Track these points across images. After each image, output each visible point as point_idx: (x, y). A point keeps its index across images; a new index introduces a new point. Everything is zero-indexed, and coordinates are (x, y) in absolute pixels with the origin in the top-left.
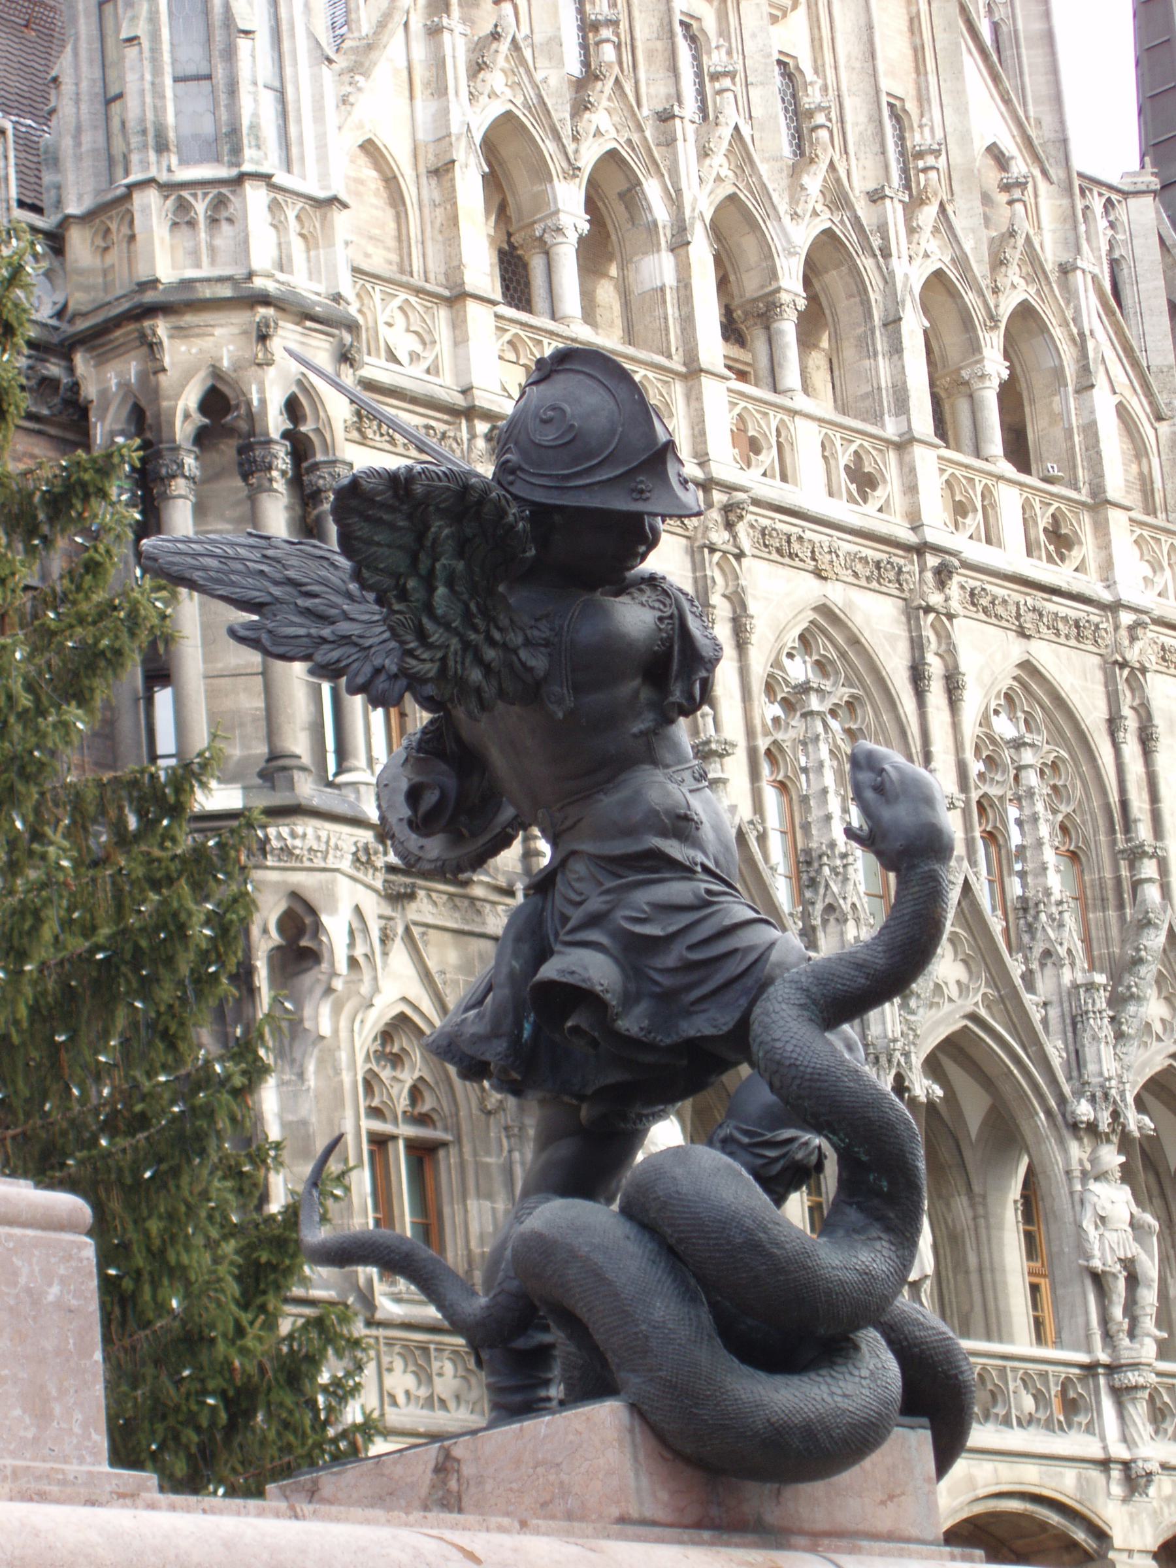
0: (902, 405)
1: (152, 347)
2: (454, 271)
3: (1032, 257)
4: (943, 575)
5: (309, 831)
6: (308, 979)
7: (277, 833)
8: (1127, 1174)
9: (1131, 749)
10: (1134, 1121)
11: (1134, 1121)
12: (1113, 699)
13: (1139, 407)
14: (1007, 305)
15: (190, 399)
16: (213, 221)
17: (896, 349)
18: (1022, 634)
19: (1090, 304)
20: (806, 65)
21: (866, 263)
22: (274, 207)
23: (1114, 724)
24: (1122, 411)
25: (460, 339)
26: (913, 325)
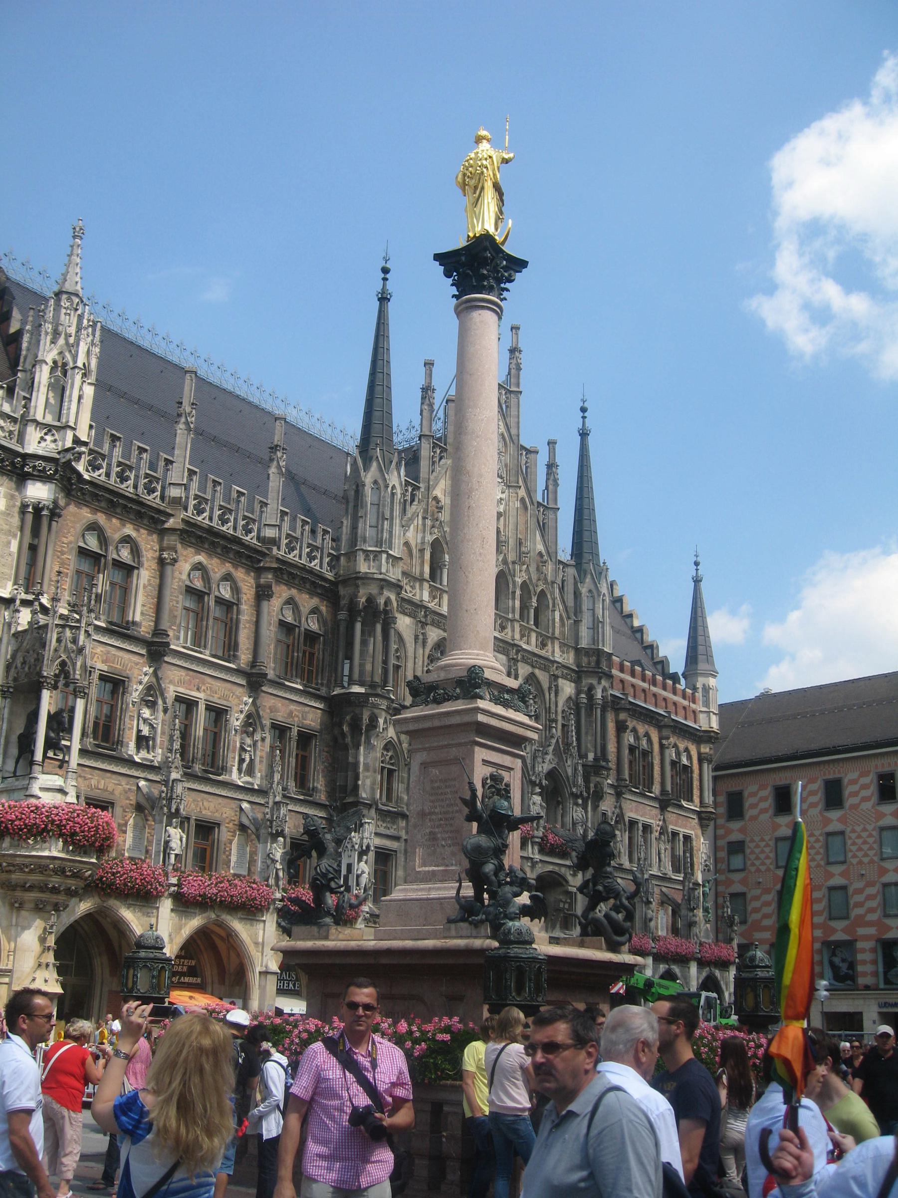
0: (513, 612)
1: (357, 586)
2: (422, 573)
3: (546, 579)
4: (518, 652)
5: (378, 701)
6: (372, 732)
7: (372, 699)
8: (540, 794)
9: (553, 695)
10: (544, 782)
11: (544, 782)
12: (550, 683)
13: (564, 615)
14: (539, 589)
15: (363, 600)
16: (374, 560)
17: (514, 599)
18: (533, 667)
19: (557, 591)
20: (502, 530)
21: (509, 578)
22: (387, 558)
23: (550, 688)
24: (561, 616)
25: (421, 589)
26: (518, 592)
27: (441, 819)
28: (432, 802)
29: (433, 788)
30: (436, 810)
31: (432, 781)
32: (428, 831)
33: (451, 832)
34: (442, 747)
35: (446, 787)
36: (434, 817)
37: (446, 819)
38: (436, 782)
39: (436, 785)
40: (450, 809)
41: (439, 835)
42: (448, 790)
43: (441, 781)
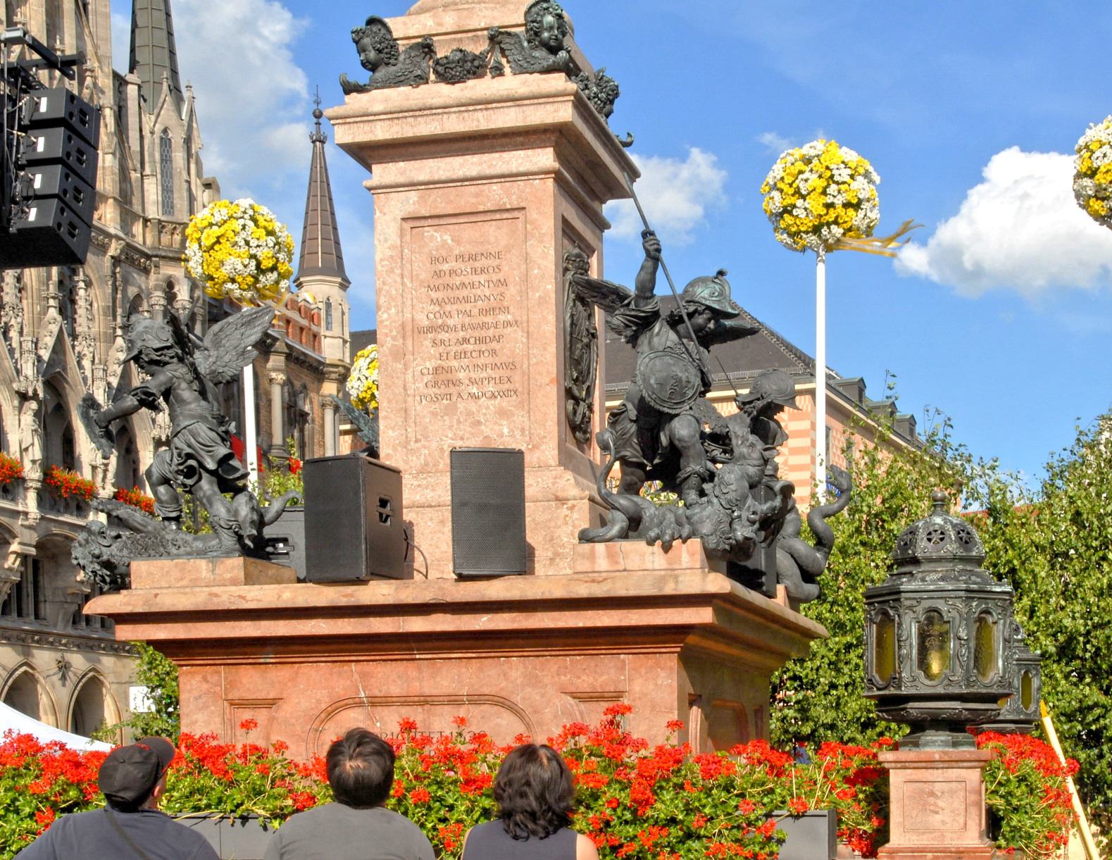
27: (466, 341)
29: (438, 274)
30: (451, 322)
31: (435, 260)
32: (430, 365)
33: (495, 366)
35: (474, 271)
36: (444, 336)
37: (481, 340)
38: (445, 260)
39: (446, 267)
42: (482, 278)
43: (460, 257)
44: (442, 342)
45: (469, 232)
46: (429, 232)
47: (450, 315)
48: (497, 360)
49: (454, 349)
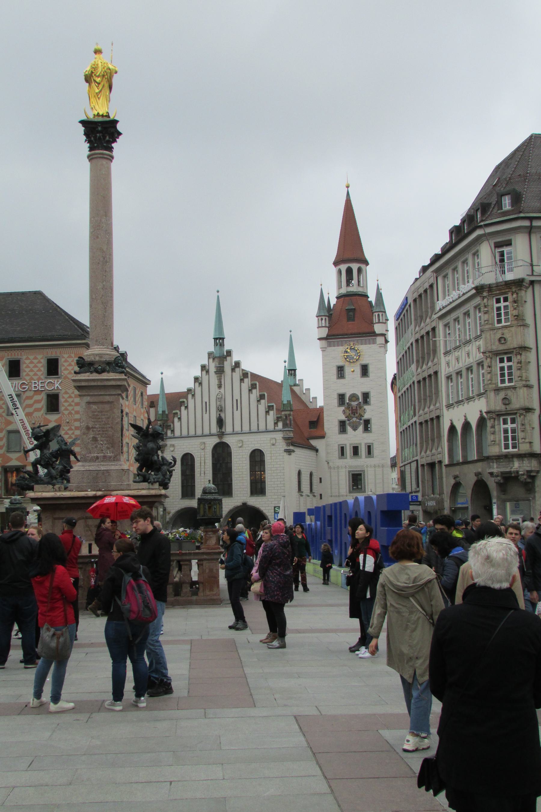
27: (100, 431)
28: (93, 422)
29: (94, 415)
30: (96, 426)
31: (93, 412)
33: (106, 437)
34: (101, 395)
35: (102, 415)
36: (95, 430)
37: (103, 431)
38: (95, 412)
39: (95, 414)
40: (105, 427)
41: (99, 439)
42: (103, 417)
43: (99, 412)
44: (94, 431)
45: (100, 406)
46: (91, 405)
47: (96, 425)
48: (106, 436)
49: (97, 433)
